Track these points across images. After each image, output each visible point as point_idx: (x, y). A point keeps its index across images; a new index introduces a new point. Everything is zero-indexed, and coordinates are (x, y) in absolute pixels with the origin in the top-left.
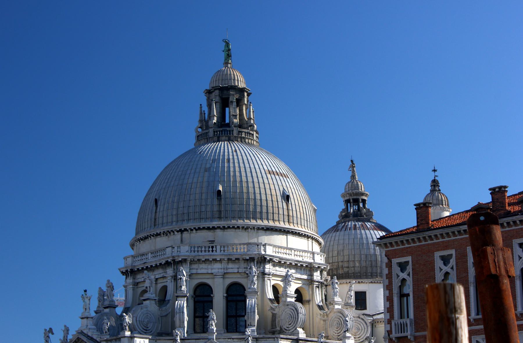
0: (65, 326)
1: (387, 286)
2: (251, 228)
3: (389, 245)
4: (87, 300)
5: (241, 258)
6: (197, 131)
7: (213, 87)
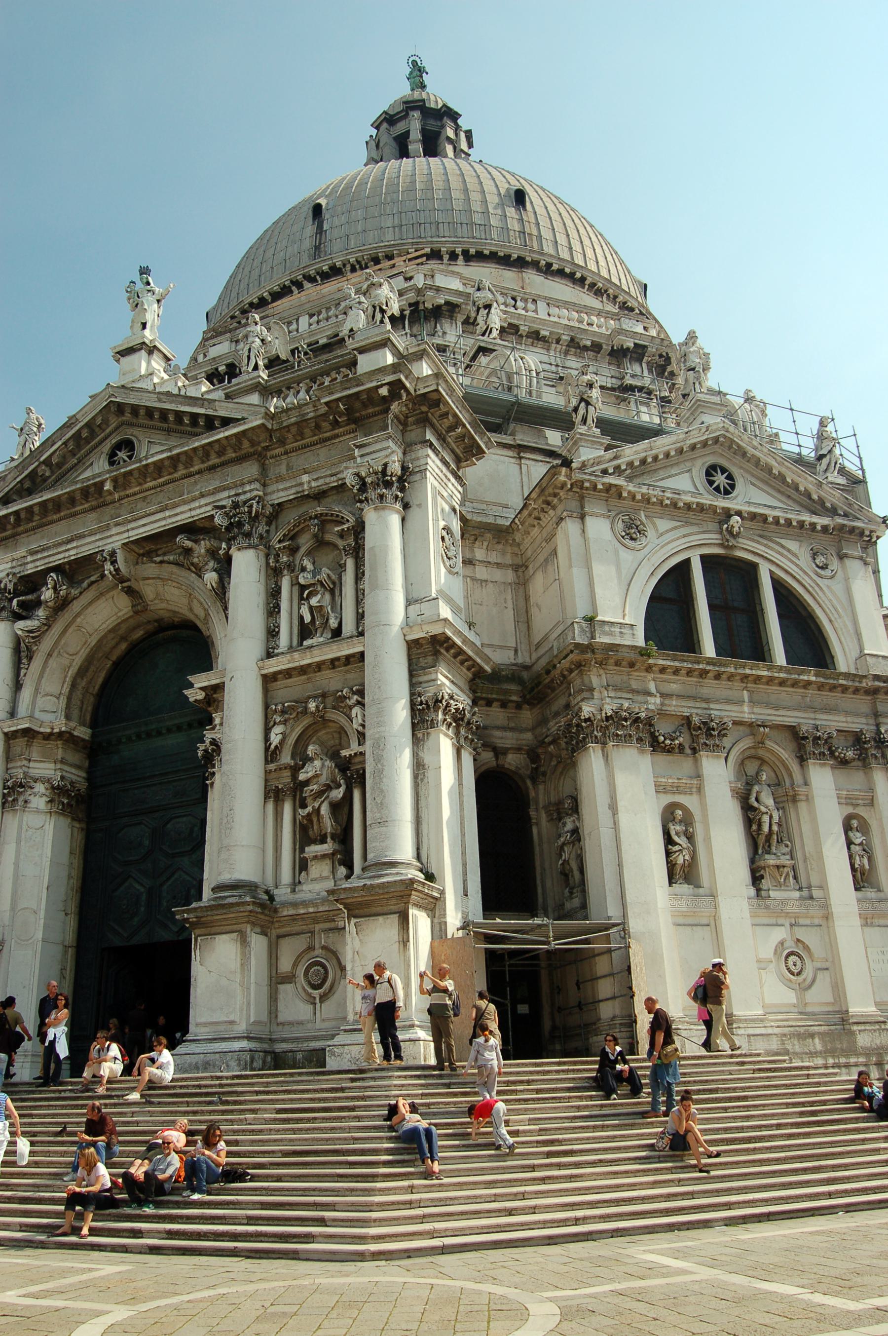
2: (608, 295)
5: (607, 345)
7: (405, 103)
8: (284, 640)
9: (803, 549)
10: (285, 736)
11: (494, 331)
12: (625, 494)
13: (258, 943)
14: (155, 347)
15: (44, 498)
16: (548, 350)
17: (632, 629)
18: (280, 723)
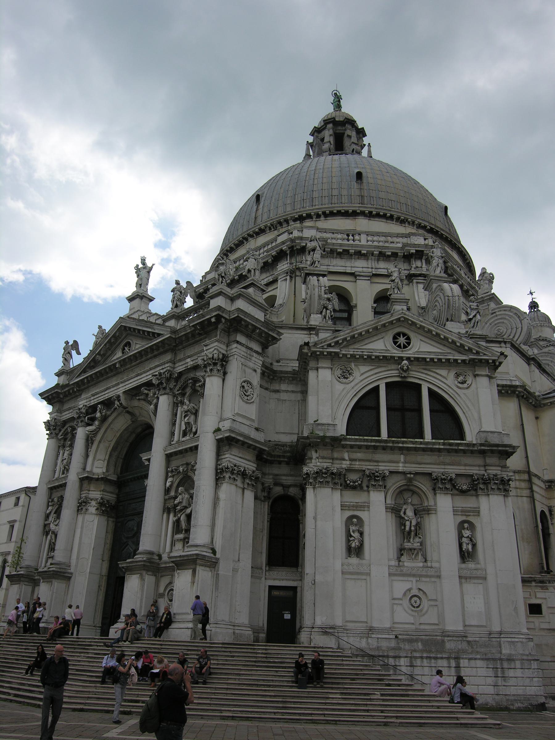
0: (100, 327)
2: (409, 223)
4: (144, 273)
5: (401, 253)
7: (324, 121)
9: (450, 374)
10: (172, 482)
11: (317, 262)
12: (341, 356)
13: (150, 579)
14: (143, 296)
15: (96, 371)
16: (368, 260)
17: (334, 427)
18: (171, 477)
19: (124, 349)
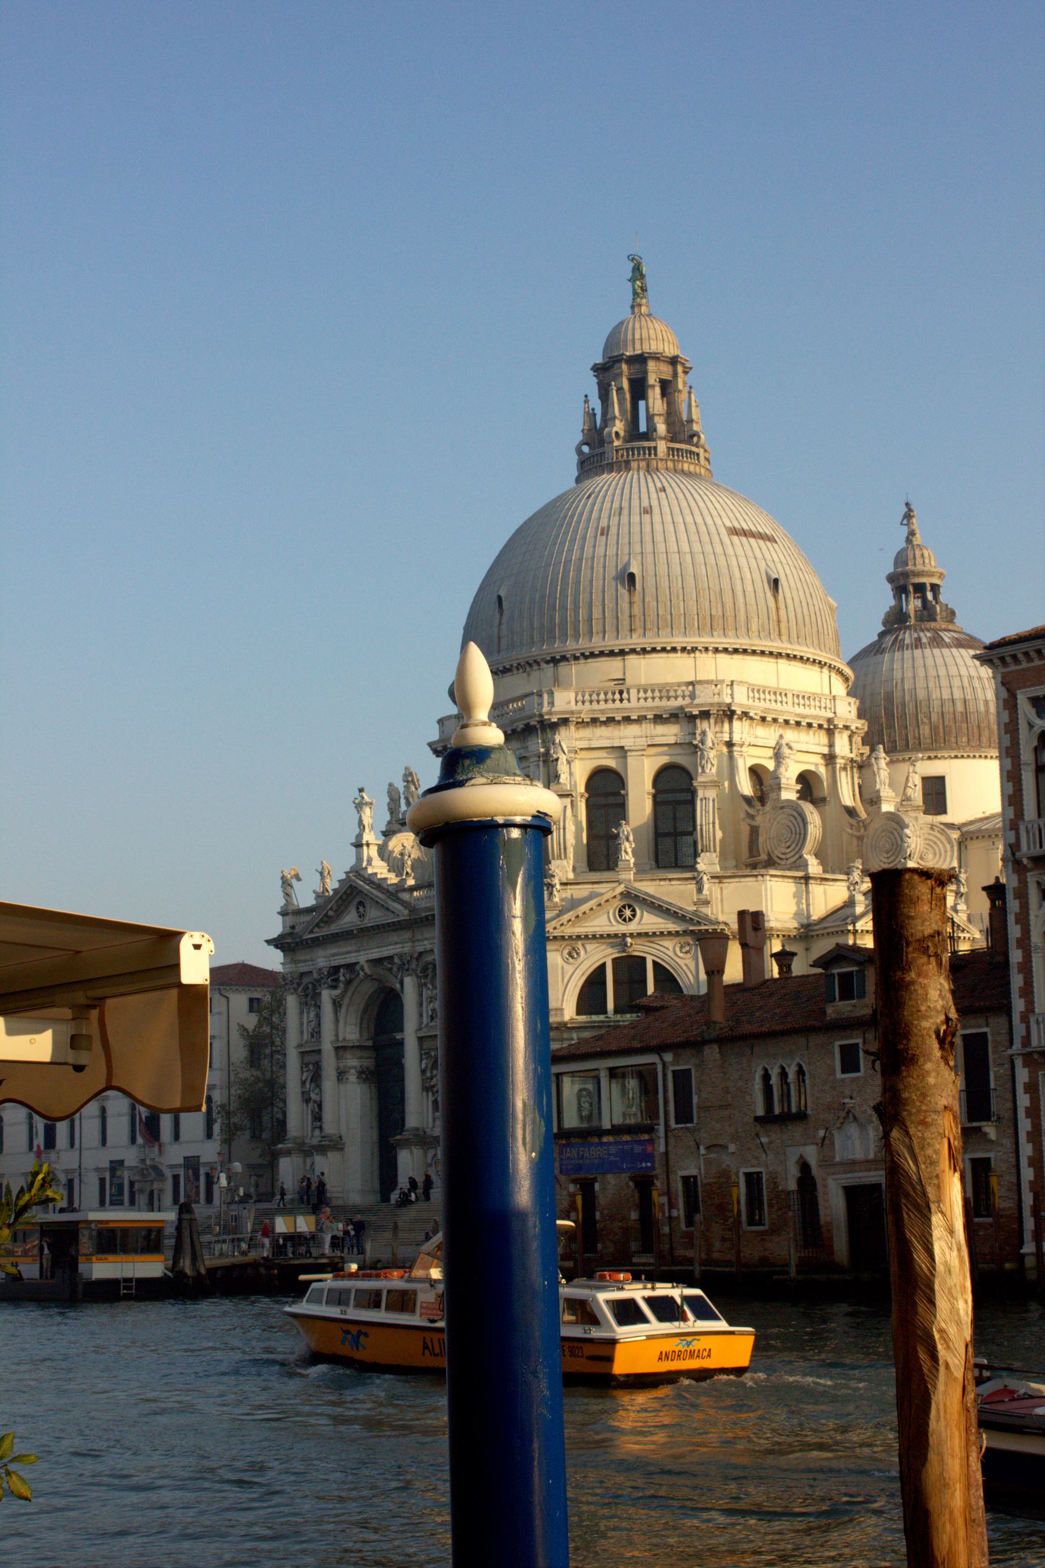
1: (1007, 748)
2: (700, 651)
3: (1009, 660)
6: (579, 451)
7: (610, 358)
8: (425, 1020)
10: (427, 1064)
13: (417, 1152)
19: (358, 908)
